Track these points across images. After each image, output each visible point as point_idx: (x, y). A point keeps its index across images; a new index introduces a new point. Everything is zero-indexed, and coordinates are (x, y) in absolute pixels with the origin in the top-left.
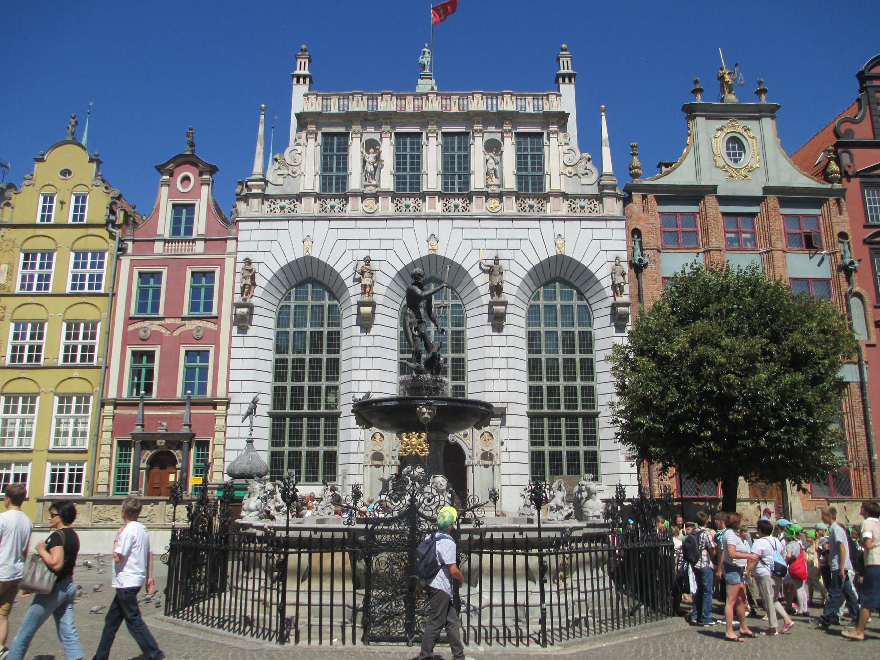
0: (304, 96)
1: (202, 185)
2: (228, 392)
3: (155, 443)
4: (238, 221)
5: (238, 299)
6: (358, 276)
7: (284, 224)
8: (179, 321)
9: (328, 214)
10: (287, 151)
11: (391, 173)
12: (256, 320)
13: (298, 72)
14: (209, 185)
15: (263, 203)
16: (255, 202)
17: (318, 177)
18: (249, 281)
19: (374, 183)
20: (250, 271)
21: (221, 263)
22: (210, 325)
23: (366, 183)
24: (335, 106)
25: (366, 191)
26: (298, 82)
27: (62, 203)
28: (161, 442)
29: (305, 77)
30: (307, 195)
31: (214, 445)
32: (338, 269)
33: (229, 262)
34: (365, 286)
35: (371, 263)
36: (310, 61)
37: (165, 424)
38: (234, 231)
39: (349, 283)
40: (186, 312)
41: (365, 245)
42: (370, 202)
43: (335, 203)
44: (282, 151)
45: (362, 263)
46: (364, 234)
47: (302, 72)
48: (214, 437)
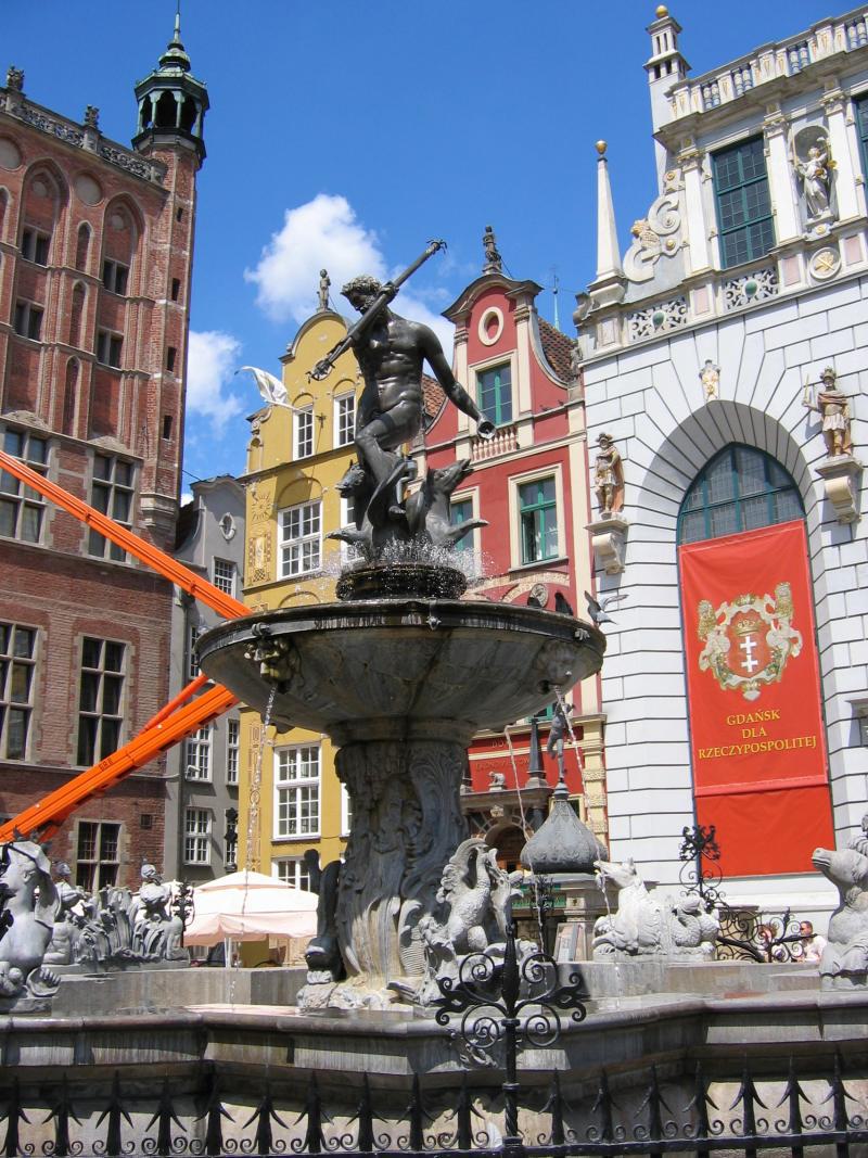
0: (670, 94)
1: (516, 321)
2: (600, 702)
3: (488, 813)
4: (582, 369)
5: (597, 518)
6: (816, 417)
7: (661, 353)
8: (506, 581)
9: (745, 306)
10: (652, 211)
11: (858, 182)
12: (633, 552)
13: (656, 58)
14: (527, 318)
15: (622, 324)
16: (608, 328)
17: (715, 241)
18: (610, 479)
19: (826, 214)
20: (609, 458)
21: (561, 456)
22: (559, 579)
23: (811, 221)
24: (726, 91)
25: (813, 236)
26: (658, 75)
27: (321, 418)
28: (497, 811)
29: (668, 62)
30: (696, 282)
31: (586, 809)
32: (774, 413)
33: (576, 452)
34: (831, 434)
35: (838, 383)
36: (677, 29)
37: (500, 776)
38: (575, 389)
39: (799, 437)
40: (516, 564)
41: (823, 347)
42: (823, 257)
43: (758, 281)
44: (644, 216)
45: (822, 388)
46: (817, 325)
47: (665, 54)
48: (582, 791)
